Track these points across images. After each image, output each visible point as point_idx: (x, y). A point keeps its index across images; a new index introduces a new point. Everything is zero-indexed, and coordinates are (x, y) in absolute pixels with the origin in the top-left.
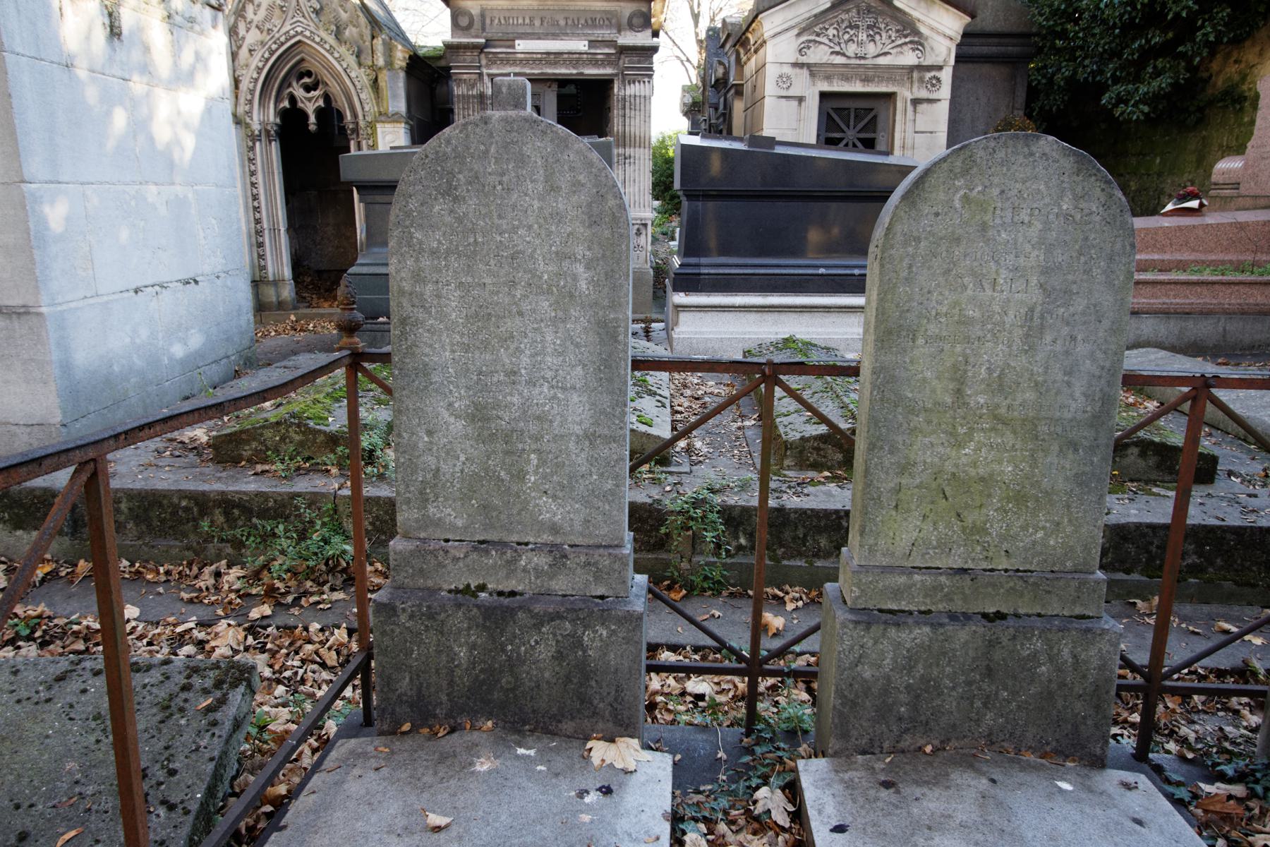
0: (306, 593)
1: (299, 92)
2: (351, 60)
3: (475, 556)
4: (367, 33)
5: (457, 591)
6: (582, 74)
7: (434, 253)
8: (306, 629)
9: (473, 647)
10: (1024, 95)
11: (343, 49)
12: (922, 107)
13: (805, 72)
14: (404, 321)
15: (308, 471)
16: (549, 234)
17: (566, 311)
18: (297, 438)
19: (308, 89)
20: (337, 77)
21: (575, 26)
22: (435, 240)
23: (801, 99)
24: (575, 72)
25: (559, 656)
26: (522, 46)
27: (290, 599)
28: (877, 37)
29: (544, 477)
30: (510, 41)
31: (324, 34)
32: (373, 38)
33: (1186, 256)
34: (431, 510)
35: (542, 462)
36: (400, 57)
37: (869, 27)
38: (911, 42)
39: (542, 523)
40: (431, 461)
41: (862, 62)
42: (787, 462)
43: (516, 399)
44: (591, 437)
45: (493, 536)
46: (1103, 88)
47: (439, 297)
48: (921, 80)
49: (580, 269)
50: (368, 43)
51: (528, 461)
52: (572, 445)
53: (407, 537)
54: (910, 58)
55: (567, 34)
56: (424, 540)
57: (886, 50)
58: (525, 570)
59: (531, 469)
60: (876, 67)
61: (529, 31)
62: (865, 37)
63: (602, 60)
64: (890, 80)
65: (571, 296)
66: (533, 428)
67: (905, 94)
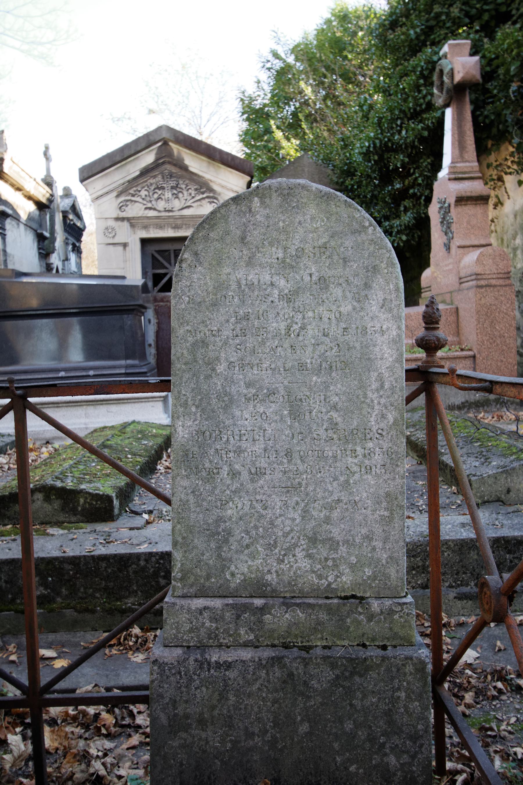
13: (126, 224)
23: (125, 245)
28: (180, 195)
37: (172, 188)
38: (208, 197)
41: (171, 214)
57: (188, 204)
60: (182, 217)
62: (170, 195)
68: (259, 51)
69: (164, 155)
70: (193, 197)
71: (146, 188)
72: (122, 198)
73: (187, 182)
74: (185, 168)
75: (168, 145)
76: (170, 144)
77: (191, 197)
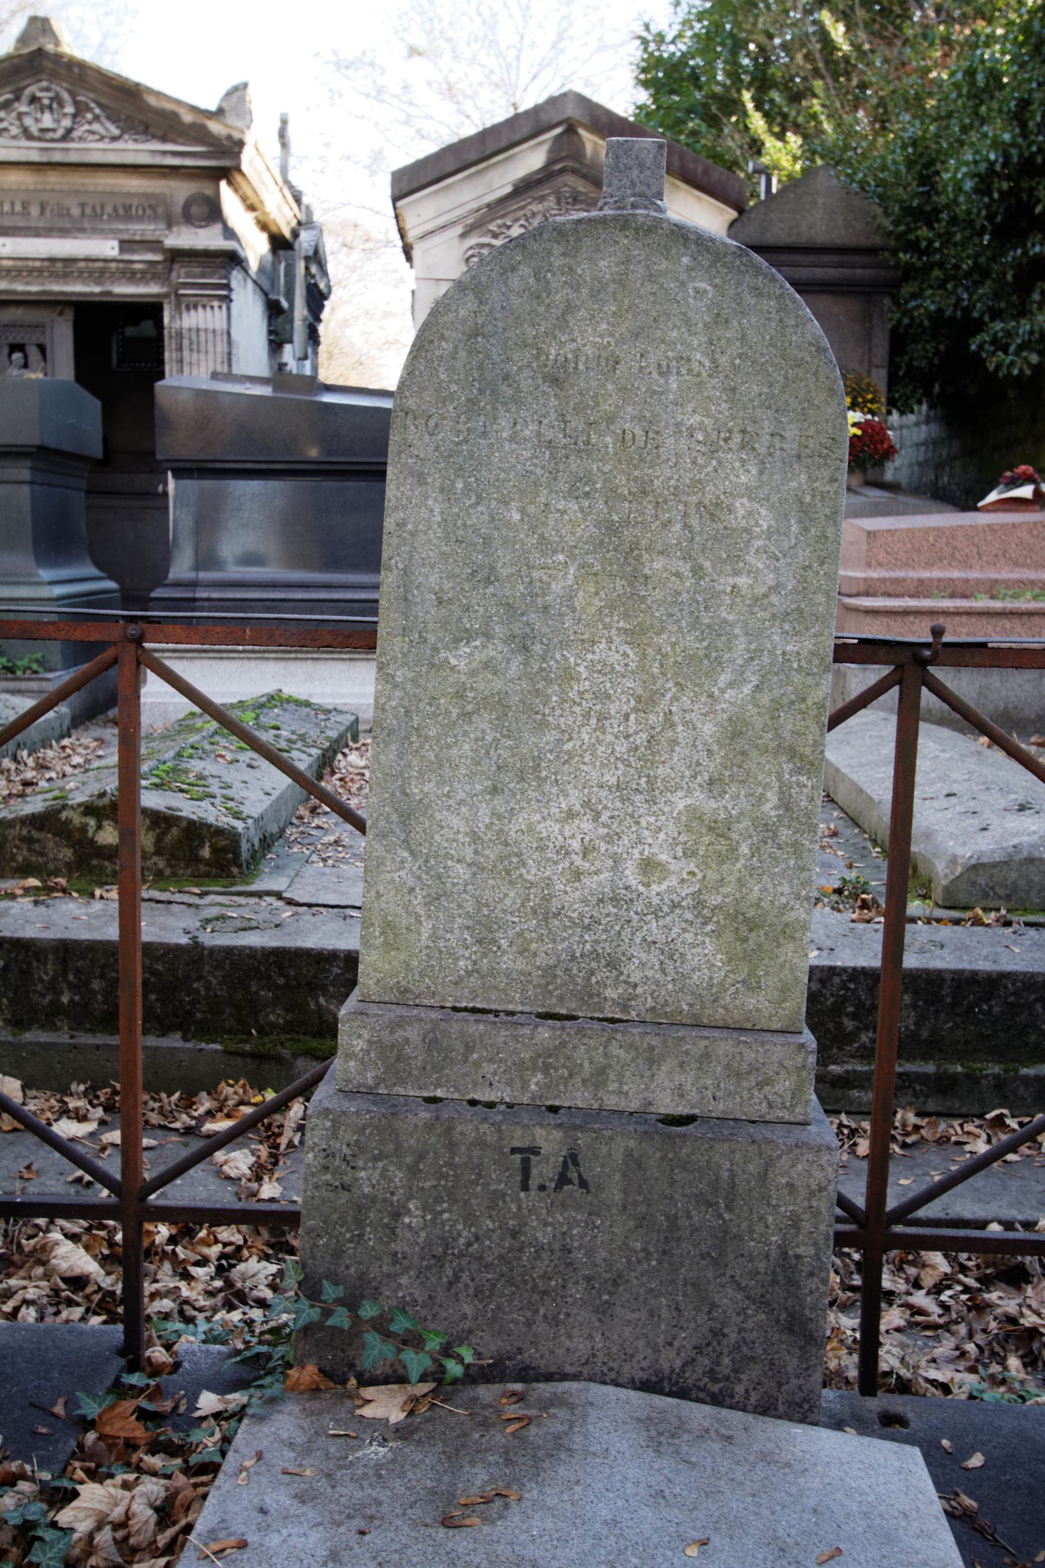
6: (109, 293)
10: (886, 344)
21: (97, 216)
24: (97, 289)
33: (1007, 574)
46: (979, 326)
55: (82, 230)
61: (21, 223)
63: (143, 272)
69: (564, 154)
71: (522, 222)
72: (473, 241)
75: (577, 133)
76: (582, 132)
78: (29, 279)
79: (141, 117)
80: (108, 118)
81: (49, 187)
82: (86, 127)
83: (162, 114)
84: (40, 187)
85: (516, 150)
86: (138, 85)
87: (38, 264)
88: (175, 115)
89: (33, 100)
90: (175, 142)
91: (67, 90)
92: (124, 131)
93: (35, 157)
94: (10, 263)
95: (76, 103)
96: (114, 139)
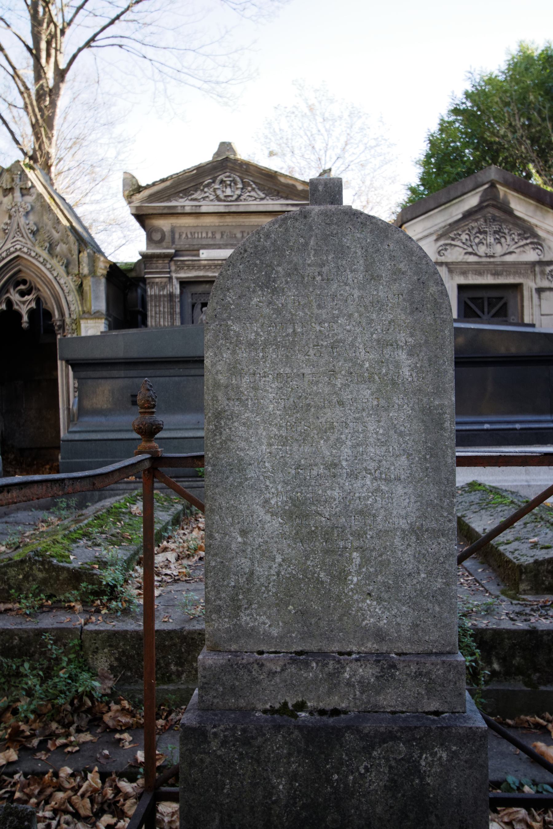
0: (53, 736)
1: (15, 297)
2: (61, 270)
3: (293, 669)
4: (75, 248)
5: (272, 711)
7: (251, 344)
8: (56, 774)
9: (294, 777)
11: (54, 262)
12: (544, 295)
14: (218, 415)
15: (51, 609)
16: (370, 321)
17: (388, 399)
18: (40, 575)
19: (22, 294)
20: (48, 283)
22: (252, 331)
25: (393, 786)
26: (205, 254)
27: (35, 742)
28: (503, 240)
29: (368, 577)
30: (195, 251)
31: (38, 250)
32: (80, 252)
34: (244, 618)
35: (366, 561)
36: (102, 269)
37: (495, 232)
38: (531, 243)
39: (366, 629)
40: (244, 563)
41: (492, 260)
42: (523, 586)
43: (336, 494)
44: (417, 532)
45: (312, 646)
47: (256, 389)
48: (543, 273)
49: (402, 356)
50: (75, 256)
51: (350, 560)
52: (397, 541)
53: (215, 649)
54: (531, 256)
56: (235, 653)
57: (511, 250)
58: (349, 684)
59: (353, 568)
60: (504, 263)
62: (492, 240)
64: (517, 273)
65: (394, 383)
66: (356, 523)
67: (530, 285)
68: (453, 92)
69: (488, 198)
70: (516, 243)
71: (467, 232)
72: (442, 242)
73: (511, 226)
74: (510, 212)
76: (498, 186)
77: (513, 243)
78: (215, 270)
79: (276, 188)
80: (258, 189)
81: (226, 224)
82: (248, 194)
83: (287, 186)
84: (221, 224)
85: (465, 196)
86: (276, 172)
87: (220, 262)
88: (294, 186)
89: (222, 182)
90: (292, 199)
91: (239, 176)
92: (267, 195)
93: (222, 209)
94: (206, 262)
95: (243, 182)
96: (262, 199)
